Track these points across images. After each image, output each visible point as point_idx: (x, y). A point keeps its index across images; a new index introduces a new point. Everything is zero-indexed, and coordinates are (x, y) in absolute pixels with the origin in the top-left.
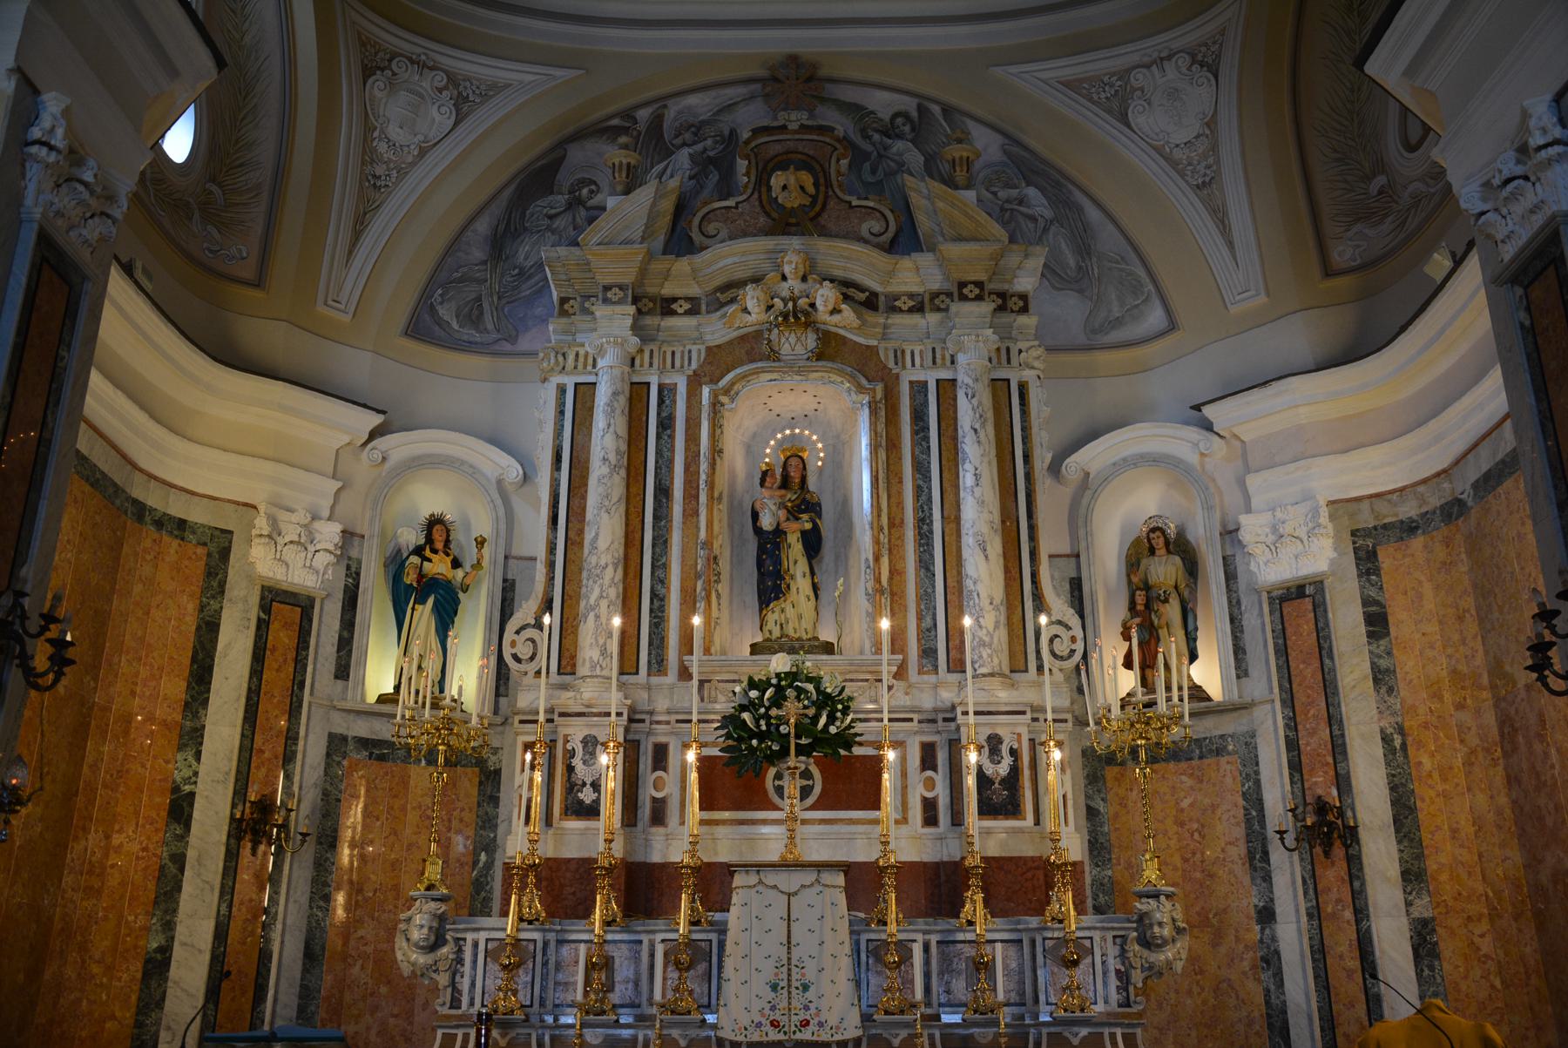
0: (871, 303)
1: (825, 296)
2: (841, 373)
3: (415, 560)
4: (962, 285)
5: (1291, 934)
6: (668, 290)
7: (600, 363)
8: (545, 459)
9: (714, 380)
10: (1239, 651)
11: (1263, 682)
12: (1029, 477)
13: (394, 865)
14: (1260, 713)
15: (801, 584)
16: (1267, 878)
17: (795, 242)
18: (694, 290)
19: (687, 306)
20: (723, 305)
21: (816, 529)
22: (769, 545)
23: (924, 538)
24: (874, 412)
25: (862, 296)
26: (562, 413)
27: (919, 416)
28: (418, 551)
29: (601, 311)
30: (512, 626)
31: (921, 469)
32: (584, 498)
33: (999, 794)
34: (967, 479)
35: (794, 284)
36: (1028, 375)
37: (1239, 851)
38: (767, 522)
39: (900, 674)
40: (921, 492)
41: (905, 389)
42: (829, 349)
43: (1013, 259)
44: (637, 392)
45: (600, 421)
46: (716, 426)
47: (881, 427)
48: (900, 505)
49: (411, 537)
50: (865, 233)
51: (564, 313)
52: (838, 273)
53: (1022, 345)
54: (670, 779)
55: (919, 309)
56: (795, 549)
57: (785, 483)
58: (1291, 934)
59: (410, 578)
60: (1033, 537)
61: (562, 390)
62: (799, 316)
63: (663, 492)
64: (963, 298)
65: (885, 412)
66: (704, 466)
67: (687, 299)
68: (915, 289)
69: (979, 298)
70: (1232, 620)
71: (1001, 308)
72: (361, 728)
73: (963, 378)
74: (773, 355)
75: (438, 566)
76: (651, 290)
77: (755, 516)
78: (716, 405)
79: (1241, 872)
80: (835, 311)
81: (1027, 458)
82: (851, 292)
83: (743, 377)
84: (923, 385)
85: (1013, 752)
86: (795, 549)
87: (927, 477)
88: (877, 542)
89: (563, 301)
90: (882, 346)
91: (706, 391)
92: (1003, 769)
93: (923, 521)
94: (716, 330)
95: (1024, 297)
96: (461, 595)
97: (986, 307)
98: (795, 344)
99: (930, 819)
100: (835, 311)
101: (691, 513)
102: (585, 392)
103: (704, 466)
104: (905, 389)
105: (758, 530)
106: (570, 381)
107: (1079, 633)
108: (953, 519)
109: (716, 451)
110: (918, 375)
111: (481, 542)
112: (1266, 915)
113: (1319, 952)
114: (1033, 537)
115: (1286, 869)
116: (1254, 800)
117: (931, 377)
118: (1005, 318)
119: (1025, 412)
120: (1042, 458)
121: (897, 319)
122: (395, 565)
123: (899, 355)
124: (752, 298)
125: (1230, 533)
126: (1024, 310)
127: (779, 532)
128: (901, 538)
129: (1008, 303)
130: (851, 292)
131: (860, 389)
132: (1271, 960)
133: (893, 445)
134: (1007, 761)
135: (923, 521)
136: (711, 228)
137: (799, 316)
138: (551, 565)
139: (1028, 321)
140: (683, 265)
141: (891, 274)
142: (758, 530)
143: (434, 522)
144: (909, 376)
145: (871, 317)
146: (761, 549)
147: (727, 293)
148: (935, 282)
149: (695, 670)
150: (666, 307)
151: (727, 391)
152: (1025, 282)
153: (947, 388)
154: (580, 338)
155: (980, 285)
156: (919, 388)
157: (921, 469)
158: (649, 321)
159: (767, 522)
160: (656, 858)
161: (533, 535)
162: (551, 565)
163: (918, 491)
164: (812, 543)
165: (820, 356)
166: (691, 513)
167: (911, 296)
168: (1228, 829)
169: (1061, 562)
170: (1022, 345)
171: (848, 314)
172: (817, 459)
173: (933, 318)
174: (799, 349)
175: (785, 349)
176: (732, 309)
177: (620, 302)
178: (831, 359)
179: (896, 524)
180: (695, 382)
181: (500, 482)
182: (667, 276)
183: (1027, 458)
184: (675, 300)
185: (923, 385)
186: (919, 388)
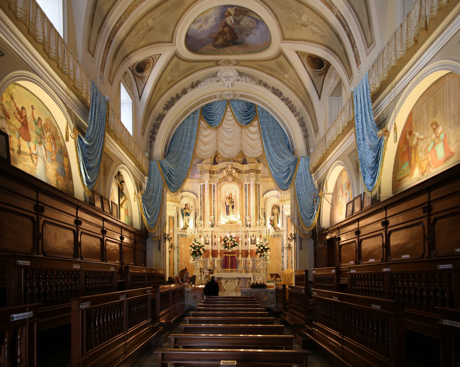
0: (240, 172)
1: (234, 171)
2: (236, 183)
3: (184, 210)
4: (251, 170)
5: (285, 259)
6: (214, 170)
7: (206, 182)
8: (199, 196)
9: (220, 184)
10: (283, 223)
11: (285, 228)
12: (259, 198)
13: (185, 250)
14: (284, 232)
15: (231, 213)
16: (283, 252)
17: (230, 163)
18: (217, 170)
19: (216, 172)
20: (221, 172)
21: (233, 205)
22: (227, 207)
23: (246, 207)
24: (240, 189)
25: (239, 171)
26: (201, 189)
27: (246, 189)
28: (185, 209)
29: (205, 174)
30: (197, 219)
31: (246, 197)
32: (204, 201)
33: (253, 242)
34: (251, 199)
35: (230, 170)
36: (260, 183)
37: (281, 249)
38: (227, 205)
39: (243, 226)
40: (246, 201)
41: (244, 185)
42: (234, 179)
43: (258, 165)
44: (210, 185)
45: (206, 191)
46: (220, 191)
47: (241, 191)
48: (243, 203)
49: (184, 207)
50: (239, 160)
51: (200, 174)
52: (236, 167)
53: (259, 178)
54: (216, 239)
55: (246, 173)
56: (230, 207)
57: (229, 198)
58: (285, 259)
59: (184, 213)
60: (259, 207)
61: (201, 185)
62: (230, 174)
63: (214, 200)
64: (252, 172)
65: (241, 188)
66: (219, 197)
67: (216, 171)
68: (246, 170)
69: (254, 172)
70: (282, 219)
71: (257, 173)
72: (180, 233)
73: (251, 184)
74: (227, 180)
75: (187, 211)
76: (211, 170)
77: (226, 203)
78: (220, 188)
79: (281, 251)
80: (235, 173)
81: (259, 195)
82: (237, 170)
83: (223, 184)
84: (246, 184)
85: (255, 237)
86: (230, 207)
87: (246, 199)
88: (240, 208)
89: (200, 172)
90: (241, 179)
91: (219, 185)
92: (254, 239)
93: (246, 205)
94: (220, 176)
95: (260, 171)
96: (190, 214)
97: (254, 173)
98: (230, 179)
99: (246, 245)
100: (235, 173)
101: (217, 204)
102: (204, 185)
103: (219, 197)
104: (244, 185)
105: (226, 205)
106: (202, 184)
107: (264, 220)
108: (250, 205)
109: (220, 195)
110: (246, 183)
111: (192, 207)
112: (283, 257)
113: (288, 261)
114: (259, 207)
115: (285, 251)
116: (283, 243)
117: (247, 183)
118: (257, 174)
119: (259, 189)
120: (261, 195)
121: (243, 174)
122: (182, 211)
123: (243, 180)
124: (225, 172)
125: (283, 207)
126: (260, 173)
127: (229, 206)
128: (243, 207)
129: (257, 172)
130: (237, 170)
131: (238, 186)
132: (283, 262)
133: (242, 194)
134: (255, 238)
135: (246, 205)
136: (219, 160)
137: (230, 174)
138: (201, 211)
139: (260, 175)
140: (215, 166)
141: (242, 167)
142: (226, 205)
143: (186, 205)
144: (245, 183)
145: (240, 174)
146: (227, 208)
147: (222, 170)
148: (248, 169)
149: (219, 225)
150: (213, 172)
151: (221, 186)
152: (260, 168)
153: (249, 185)
154: (203, 177)
155: (254, 170)
156: (246, 185)
157: (246, 197)
158: (211, 175)
159: (227, 205)
160: (215, 249)
161: (199, 207)
162: (201, 211)
163: (245, 200)
164: (233, 207)
165: (233, 180)
166: (217, 204)
167: (245, 170)
168: (280, 246)
169: (263, 210)
170: (259, 178)
171: (237, 174)
172: (233, 195)
173: (248, 174)
174: (231, 179)
175: (229, 179)
176: (222, 173)
177: (208, 173)
178: (235, 181)
179: (242, 205)
180: (217, 184)
181: (194, 199)
182: (213, 168)
183: (259, 195)
184: (214, 171)
185: (246, 184)
186: (246, 185)
